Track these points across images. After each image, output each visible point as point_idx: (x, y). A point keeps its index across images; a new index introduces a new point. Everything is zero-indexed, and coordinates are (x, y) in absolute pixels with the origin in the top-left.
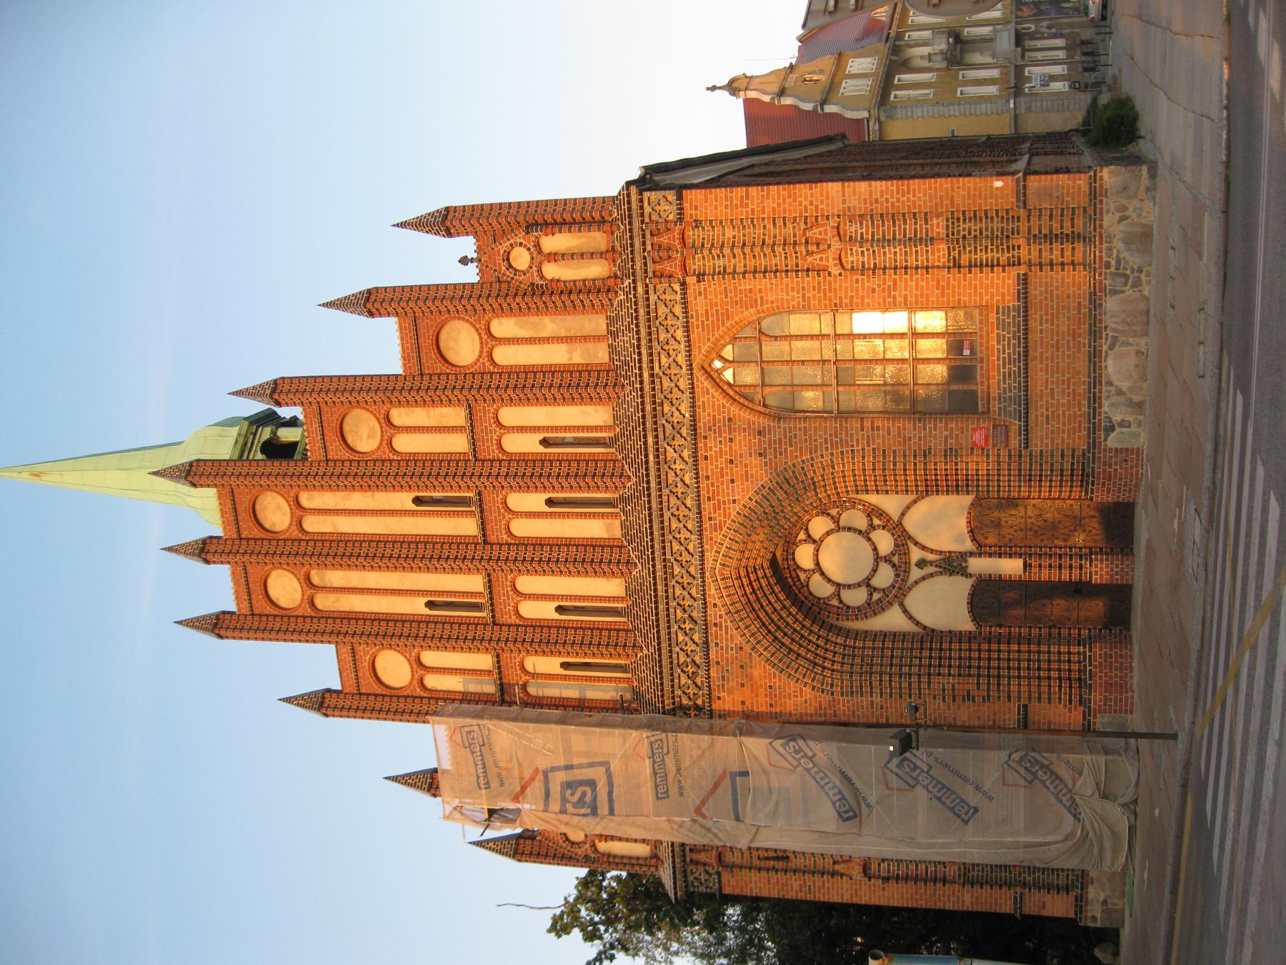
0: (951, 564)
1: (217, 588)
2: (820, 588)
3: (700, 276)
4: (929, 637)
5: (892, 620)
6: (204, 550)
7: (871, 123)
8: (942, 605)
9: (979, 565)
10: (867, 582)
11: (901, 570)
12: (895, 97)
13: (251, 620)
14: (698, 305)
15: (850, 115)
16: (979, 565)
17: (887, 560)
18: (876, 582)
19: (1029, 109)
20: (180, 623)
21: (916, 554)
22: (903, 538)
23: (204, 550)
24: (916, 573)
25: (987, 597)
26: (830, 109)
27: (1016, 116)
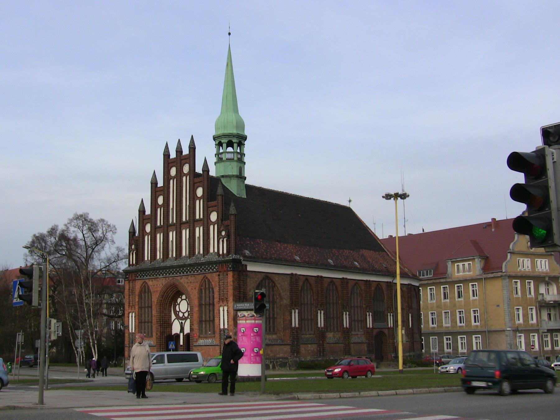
0: (182, 329)
1: (173, 155)
2: (179, 300)
3: (219, 275)
4: (170, 325)
5: (173, 317)
6: (179, 151)
7: (500, 274)
8: (176, 329)
9: (182, 334)
10: (180, 311)
11: (182, 319)
12: (516, 282)
13: (168, 162)
14: (214, 274)
15: (504, 264)
16: (182, 334)
17: (183, 315)
18: (180, 313)
19: (507, 336)
20: (167, 144)
21: (183, 322)
22: (186, 319)
23: (179, 151)
24: (180, 321)
25: (177, 336)
26: (509, 255)
27: (504, 331)
